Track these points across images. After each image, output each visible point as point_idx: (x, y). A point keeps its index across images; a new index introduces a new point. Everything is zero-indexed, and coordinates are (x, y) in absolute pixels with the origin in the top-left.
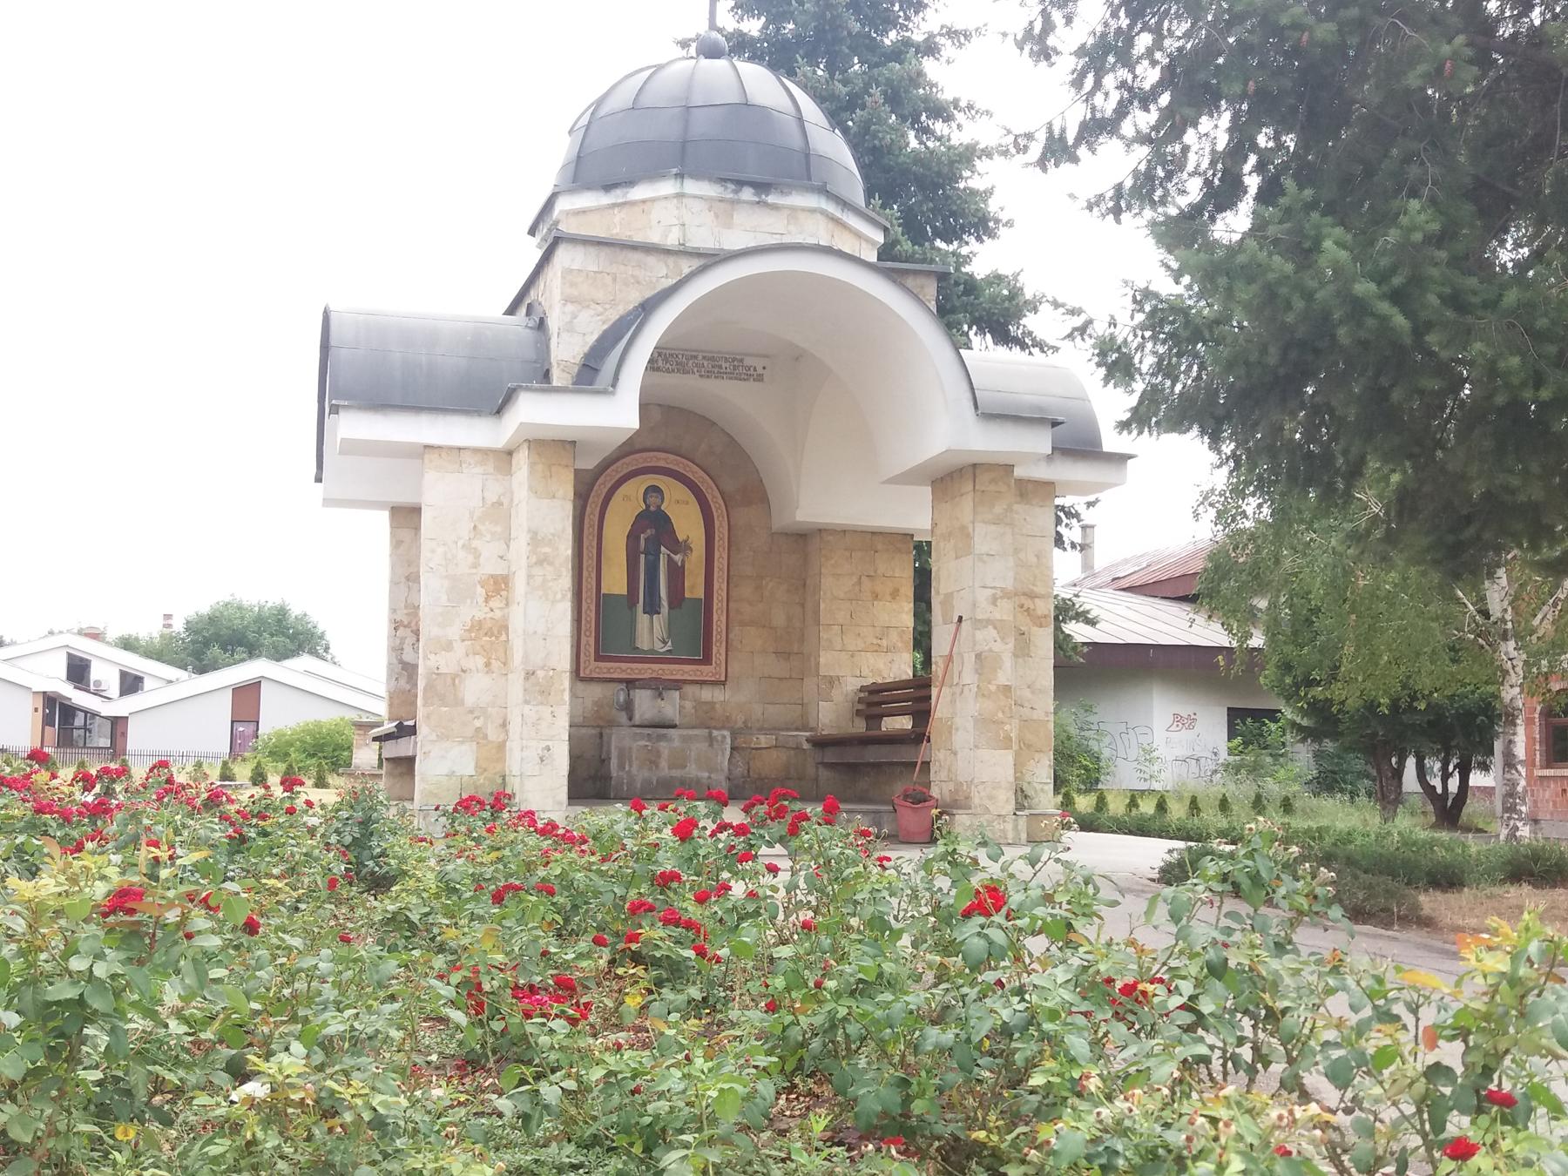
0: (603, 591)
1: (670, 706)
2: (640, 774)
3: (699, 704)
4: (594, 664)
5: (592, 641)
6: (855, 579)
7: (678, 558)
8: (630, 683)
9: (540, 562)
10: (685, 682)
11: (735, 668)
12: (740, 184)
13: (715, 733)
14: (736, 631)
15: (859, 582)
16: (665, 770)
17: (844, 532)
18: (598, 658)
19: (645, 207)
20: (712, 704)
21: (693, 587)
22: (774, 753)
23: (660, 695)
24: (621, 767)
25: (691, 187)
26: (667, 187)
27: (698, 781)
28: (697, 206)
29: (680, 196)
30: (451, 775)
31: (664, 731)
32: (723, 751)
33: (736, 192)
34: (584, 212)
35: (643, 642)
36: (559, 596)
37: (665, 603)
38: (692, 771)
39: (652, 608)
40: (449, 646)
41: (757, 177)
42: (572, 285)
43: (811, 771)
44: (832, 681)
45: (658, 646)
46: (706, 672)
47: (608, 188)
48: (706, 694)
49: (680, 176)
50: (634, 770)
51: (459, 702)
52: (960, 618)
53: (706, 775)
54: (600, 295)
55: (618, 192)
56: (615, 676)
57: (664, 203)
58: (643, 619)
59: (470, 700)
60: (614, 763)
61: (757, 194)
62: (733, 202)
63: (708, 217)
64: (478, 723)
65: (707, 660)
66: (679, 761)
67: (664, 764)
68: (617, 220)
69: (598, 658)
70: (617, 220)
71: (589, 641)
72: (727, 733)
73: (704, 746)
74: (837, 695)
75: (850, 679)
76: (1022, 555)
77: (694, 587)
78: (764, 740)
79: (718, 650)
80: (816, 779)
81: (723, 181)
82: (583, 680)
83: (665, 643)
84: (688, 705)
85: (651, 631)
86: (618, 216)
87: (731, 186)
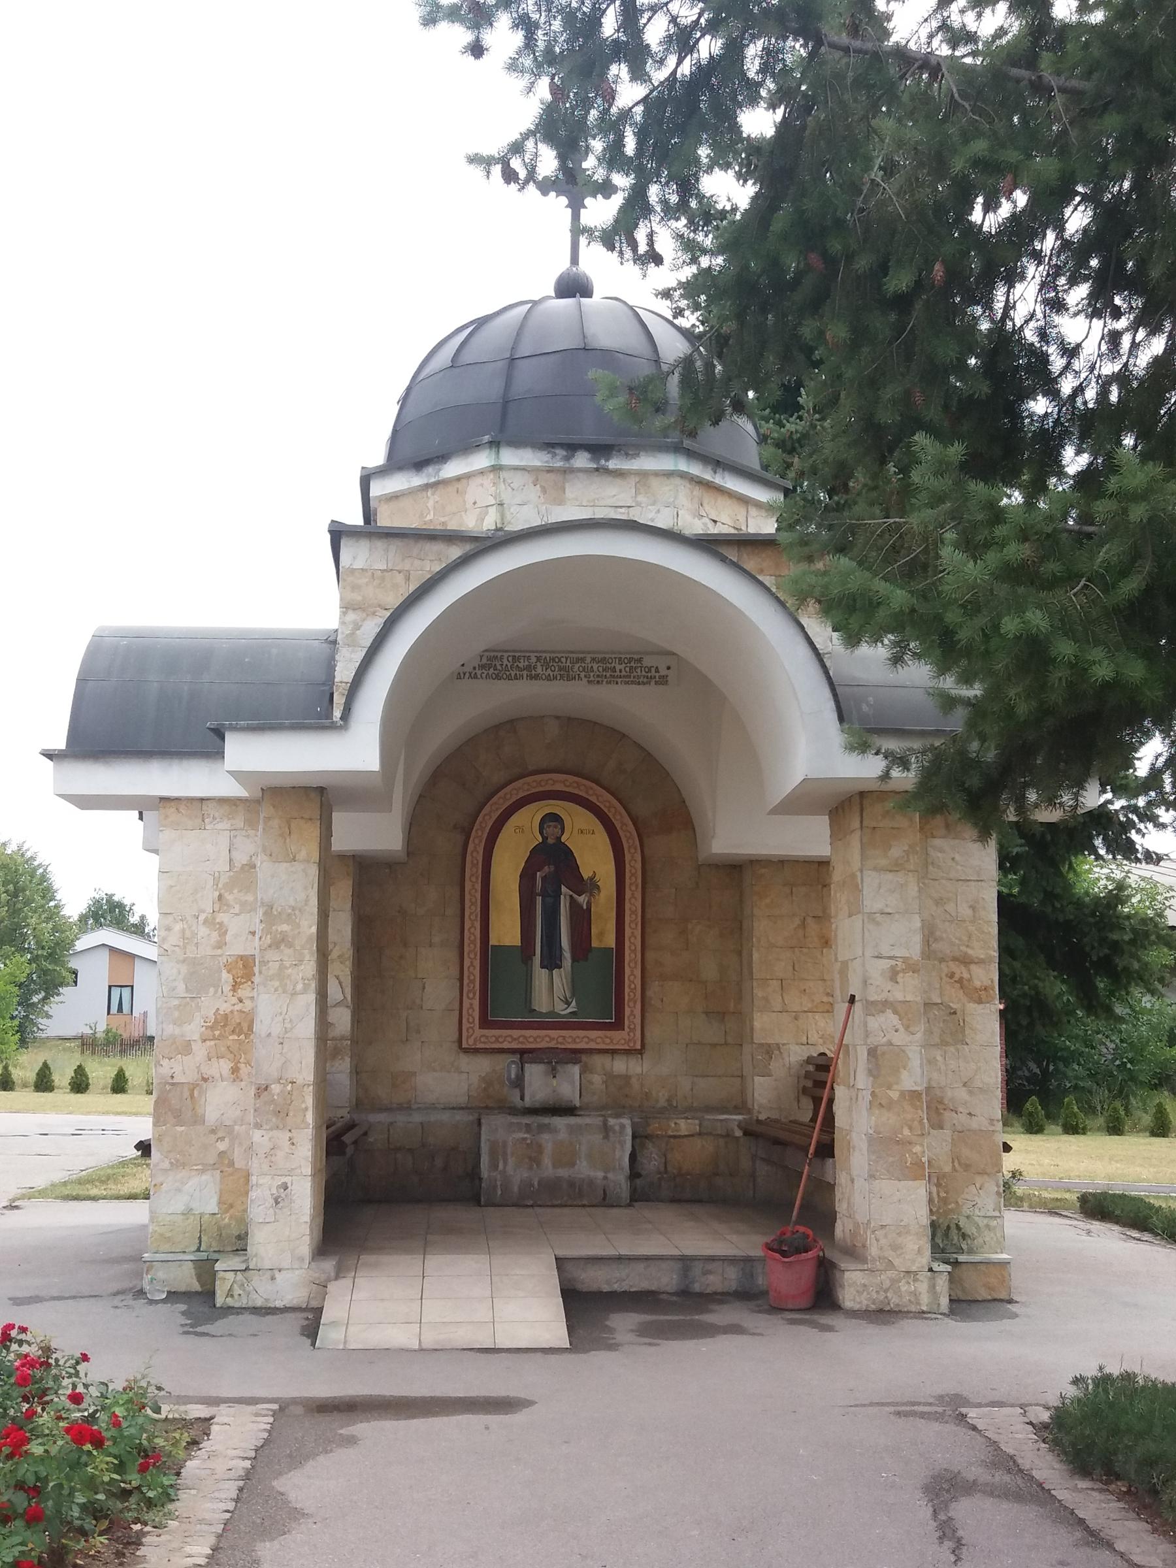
0: (493, 941)
1: (567, 1085)
2: (516, 1173)
3: (610, 1077)
4: (479, 1032)
5: (476, 1003)
6: (797, 921)
8: (525, 1055)
10: (591, 1051)
11: (655, 1032)
12: (572, 448)
13: (612, 1121)
14: (654, 989)
15: (803, 925)
16: (548, 1169)
17: (782, 863)
18: (485, 1023)
19: (460, 486)
20: (627, 1078)
21: (601, 934)
22: (698, 1142)
23: (554, 1069)
24: (494, 1166)
25: (510, 457)
26: (481, 460)
27: (591, 1182)
28: (518, 479)
29: (496, 469)
30: (188, 1212)
31: (546, 1120)
32: (622, 1143)
33: (567, 458)
35: (542, 1002)
36: (300, 987)
37: (567, 954)
38: (584, 1169)
39: (552, 961)
40: (186, 1048)
41: (591, 438)
43: (745, 1163)
44: (770, 1051)
45: (560, 1008)
46: (617, 1039)
48: (620, 1066)
49: (495, 444)
50: (510, 1170)
53: (600, 1174)
56: (506, 1045)
57: (479, 480)
58: (540, 976)
60: (485, 1160)
61: (595, 459)
62: (567, 472)
63: (533, 493)
65: (618, 1025)
66: (566, 1157)
67: (547, 1161)
68: (430, 504)
69: (485, 1023)
70: (430, 504)
71: (473, 1004)
72: (626, 1122)
73: (597, 1138)
74: (774, 1066)
75: (797, 1048)
76: (950, 907)
77: (603, 935)
78: (684, 1126)
79: (632, 1011)
80: (753, 1176)
81: (549, 446)
82: (467, 1051)
83: (568, 1004)
84: (597, 1079)
85: (551, 990)
86: (432, 499)
87: (561, 452)
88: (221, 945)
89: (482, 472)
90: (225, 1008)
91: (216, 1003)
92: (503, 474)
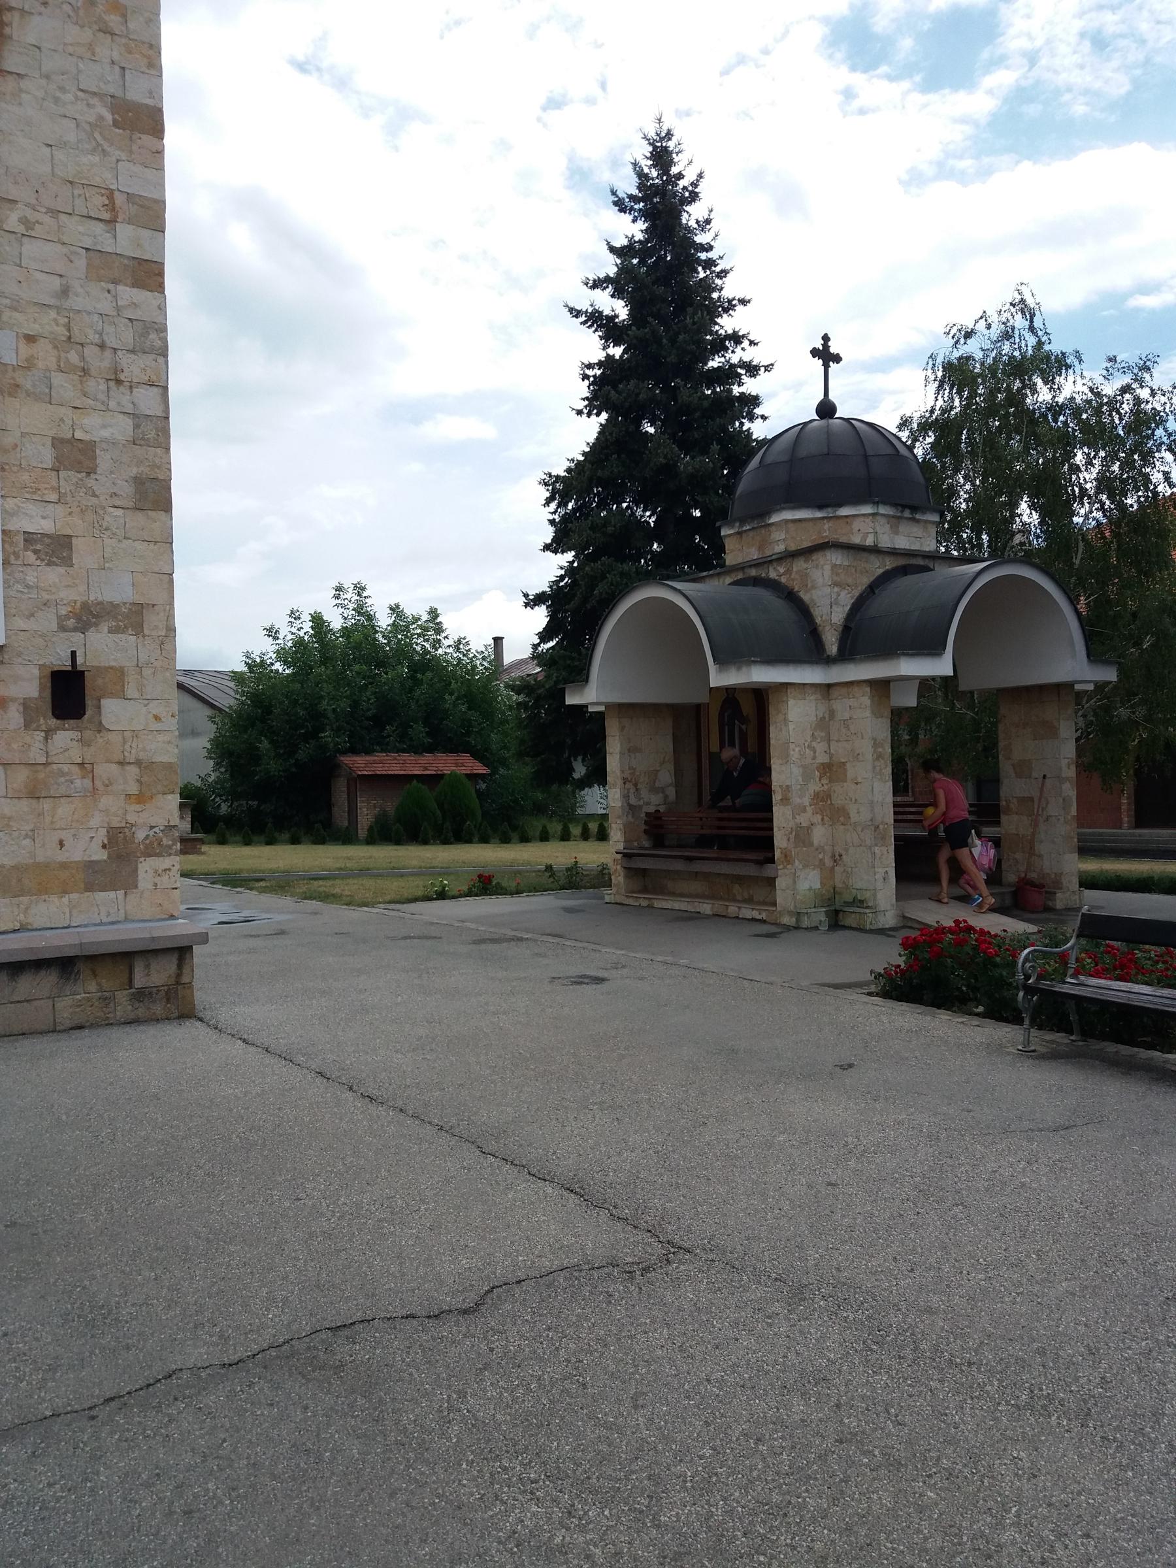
7: (744, 727)
9: (877, 759)
12: (904, 507)
25: (883, 510)
26: (868, 509)
28: (883, 520)
29: (873, 515)
33: (902, 512)
34: (800, 520)
42: (838, 574)
47: (820, 507)
49: (876, 503)
51: (811, 844)
52: (1044, 777)
54: (850, 581)
55: (830, 510)
57: (862, 519)
59: (816, 843)
64: (821, 856)
68: (826, 527)
70: (826, 527)
81: (895, 505)
88: (814, 758)
89: (864, 515)
90: (817, 789)
91: (814, 787)
92: (878, 518)
